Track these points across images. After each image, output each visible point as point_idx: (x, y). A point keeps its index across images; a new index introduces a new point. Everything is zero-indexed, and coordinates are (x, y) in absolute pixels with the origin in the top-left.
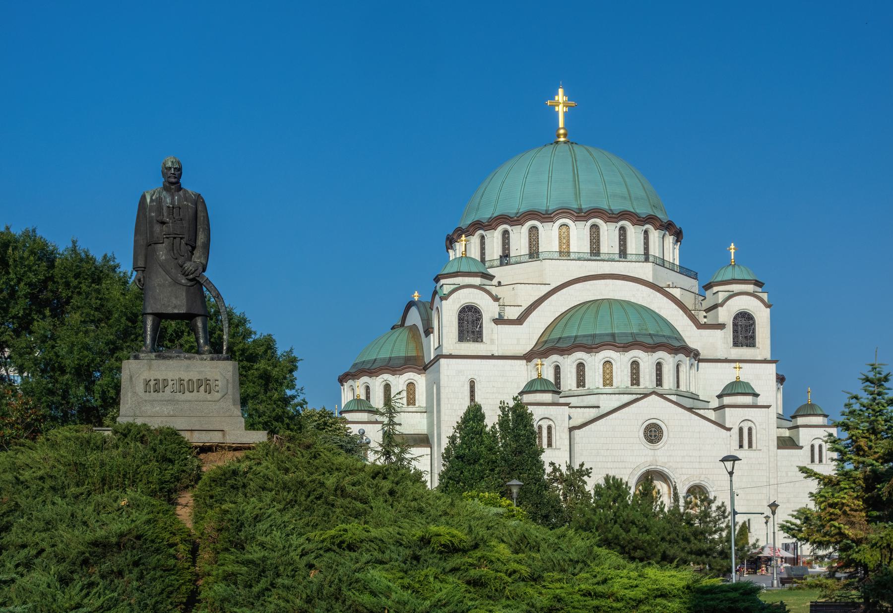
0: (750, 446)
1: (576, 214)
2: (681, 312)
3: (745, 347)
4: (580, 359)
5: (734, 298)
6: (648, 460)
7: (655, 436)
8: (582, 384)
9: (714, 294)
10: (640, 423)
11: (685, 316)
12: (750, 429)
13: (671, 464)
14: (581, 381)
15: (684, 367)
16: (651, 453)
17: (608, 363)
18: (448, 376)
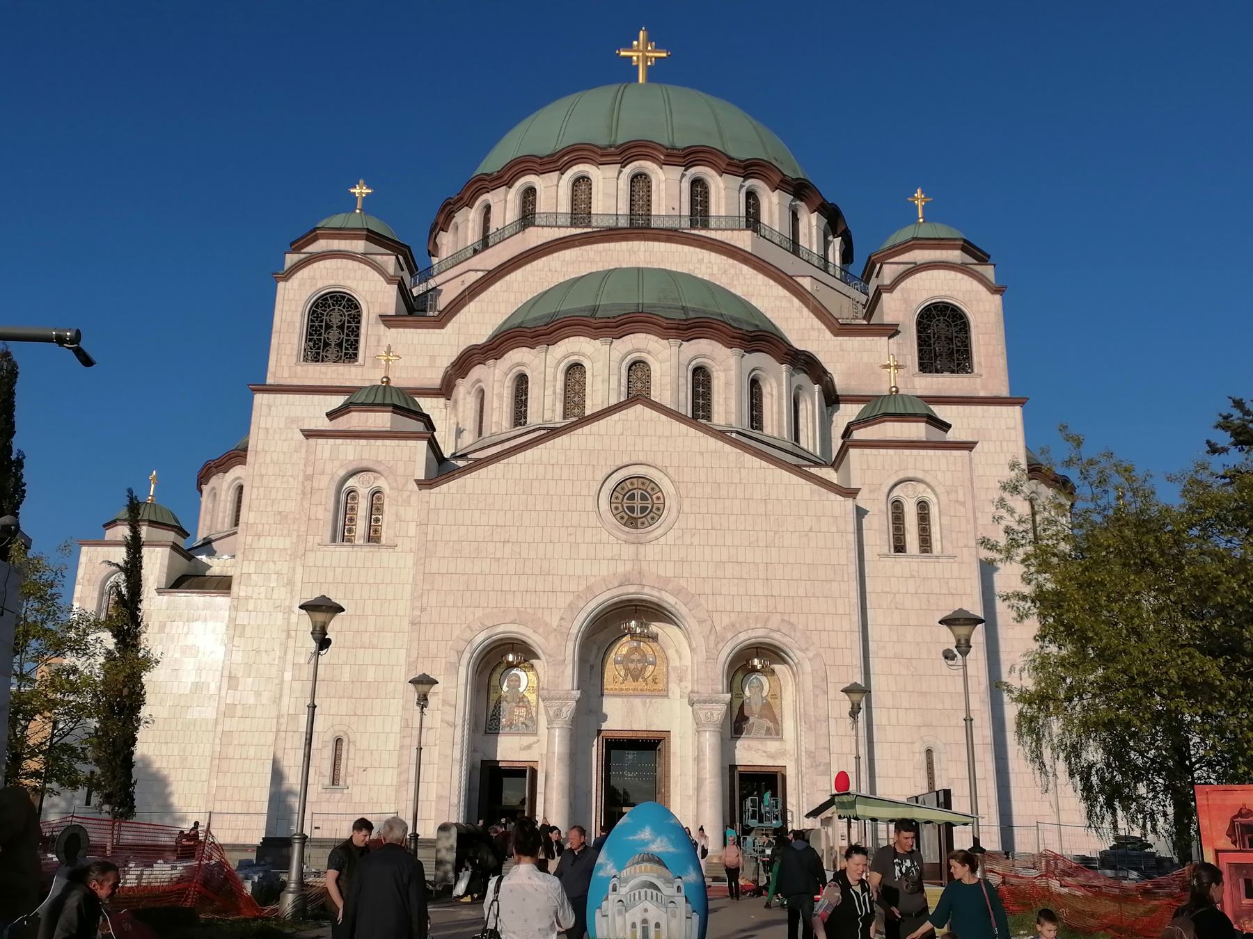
0: (925, 542)
1: (599, 151)
2: (796, 302)
3: (946, 374)
4: (518, 365)
5: (918, 275)
6: (621, 569)
7: (643, 509)
8: (523, 421)
9: (877, 276)
10: (600, 476)
11: (805, 310)
12: (923, 506)
13: (683, 583)
14: (519, 416)
15: (774, 384)
16: (628, 551)
17: (575, 370)
18: (267, 429)
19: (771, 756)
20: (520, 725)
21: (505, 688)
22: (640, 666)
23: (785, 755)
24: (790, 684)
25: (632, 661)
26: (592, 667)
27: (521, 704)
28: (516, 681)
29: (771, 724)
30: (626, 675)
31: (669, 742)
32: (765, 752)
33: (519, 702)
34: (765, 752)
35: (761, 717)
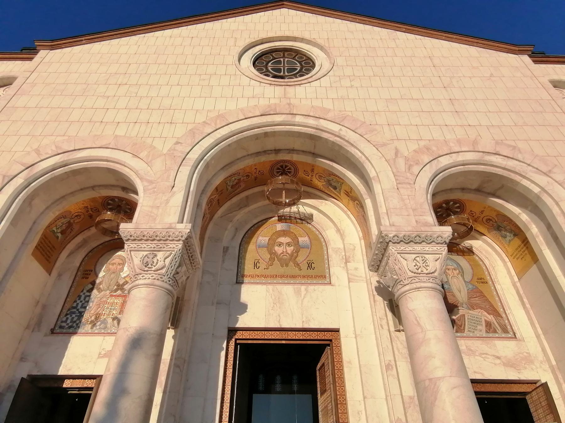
19: (509, 364)
20: (110, 320)
21: (101, 274)
22: (290, 249)
23: (532, 362)
24: (500, 262)
25: (280, 245)
26: (226, 250)
27: (119, 292)
28: (119, 264)
29: (491, 318)
30: (272, 260)
31: (339, 347)
32: (498, 358)
33: (116, 291)
34: (498, 358)
35: (472, 307)
